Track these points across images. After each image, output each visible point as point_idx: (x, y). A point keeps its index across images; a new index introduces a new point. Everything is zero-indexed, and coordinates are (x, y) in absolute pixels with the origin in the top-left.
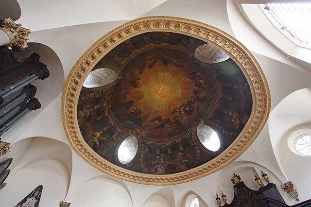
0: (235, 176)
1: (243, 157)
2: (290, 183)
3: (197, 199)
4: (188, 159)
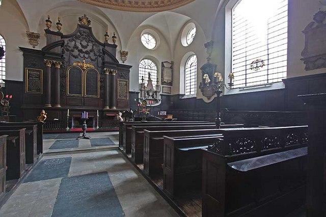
2: (127, 53)
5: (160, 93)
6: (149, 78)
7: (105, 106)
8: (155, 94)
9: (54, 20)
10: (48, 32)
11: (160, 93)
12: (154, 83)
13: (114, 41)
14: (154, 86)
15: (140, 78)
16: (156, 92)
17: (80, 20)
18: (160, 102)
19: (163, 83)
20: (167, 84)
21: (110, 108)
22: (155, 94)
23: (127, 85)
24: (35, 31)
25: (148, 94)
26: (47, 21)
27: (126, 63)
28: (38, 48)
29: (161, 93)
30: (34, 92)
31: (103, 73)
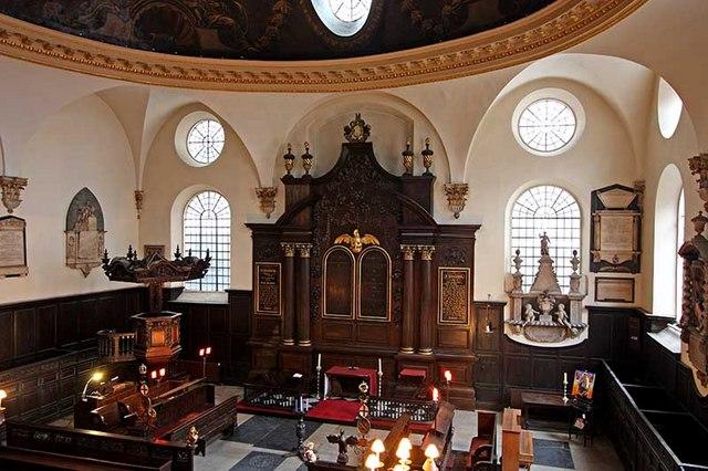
0: (359, 121)
1: (401, 92)
2: (465, 189)
3: (219, 126)
4: (235, 18)
5: (585, 303)
6: (544, 251)
7: (402, 345)
8: (562, 307)
9: (298, 152)
10: (288, 180)
11: (585, 303)
12: (564, 272)
13: (427, 164)
14: (559, 272)
15: (509, 254)
16: (566, 301)
17: (348, 131)
18: (584, 335)
19: (596, 266)
20: (615, 267)
21: (416, 351)
22: (562, 307)
23: (467, 282)
24: (267, 182)
25: (536, 307)
26: (286, 157)
27: (465, 219)
28: (273, 220)
29: (589, 301)
30: (268, 311)
31: (399, 256)
